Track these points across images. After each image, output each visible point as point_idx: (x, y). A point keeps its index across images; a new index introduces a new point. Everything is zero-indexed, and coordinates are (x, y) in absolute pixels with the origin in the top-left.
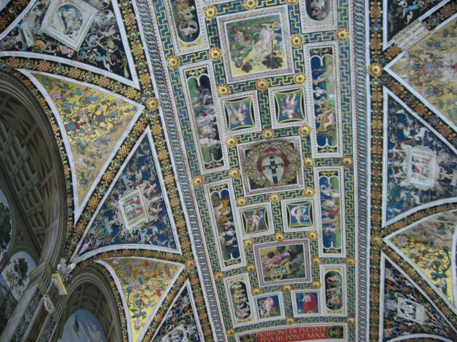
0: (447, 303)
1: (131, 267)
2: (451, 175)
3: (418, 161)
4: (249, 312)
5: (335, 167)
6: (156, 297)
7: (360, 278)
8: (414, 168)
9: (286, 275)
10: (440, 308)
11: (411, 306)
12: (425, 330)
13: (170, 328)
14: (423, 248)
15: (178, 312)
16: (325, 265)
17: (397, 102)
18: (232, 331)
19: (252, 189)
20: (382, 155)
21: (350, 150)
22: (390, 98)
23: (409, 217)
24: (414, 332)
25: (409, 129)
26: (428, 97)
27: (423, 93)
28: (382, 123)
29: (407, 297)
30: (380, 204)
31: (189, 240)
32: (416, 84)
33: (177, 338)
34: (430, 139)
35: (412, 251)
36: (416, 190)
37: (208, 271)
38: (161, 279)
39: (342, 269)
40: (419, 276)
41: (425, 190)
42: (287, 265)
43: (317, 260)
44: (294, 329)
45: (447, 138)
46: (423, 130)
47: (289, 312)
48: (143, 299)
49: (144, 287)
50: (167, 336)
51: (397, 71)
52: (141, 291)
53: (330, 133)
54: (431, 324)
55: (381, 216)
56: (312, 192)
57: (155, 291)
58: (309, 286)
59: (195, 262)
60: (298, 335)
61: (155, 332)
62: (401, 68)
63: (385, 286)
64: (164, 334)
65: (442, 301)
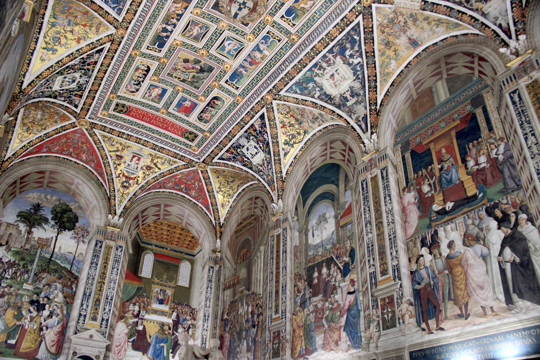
0: (282, 163)
1: (71, 8)
2: (351, 98)
3: (338, 74)
4: (137, 90)
5: (282, 36)
6: (74, 43)
7: (236, 113)
8: (332, 75)
9: (186, 80)
10: (275, 163)
11: (256, 150)
12: (254, 169)
13: (69, 72)
14: (293, 122)
15: (84, 62)
16: (219, 91)
17: (360, 31)
18: (115, 96)
19: (212, 8)
20: (320, 52)
21: (303, 34)
22: (358, 24)
23: (302, 100)
24: (245, 165)
25: (351, 52)
26: (380, 44)
27: (380, 39)
28: (339, 34)
29: (258, 144)
30: (291, 80)
31: (135, 15)
32: (381, 30)
33: (69, 82)
34: (358, 69)
35: (285, 119)
36: (322, 89)
37: (130, 46)
38: (88, 30)
39: (228, 100)
40: (277, 137)
41: (327, 93)
42: (192, 74)
43: (216, 84)
44: (162, 118)
45: (369, 77)
46: (359, 59)
47: (167, 105)
48: (61, 38)
49: (69, 29)
50: (63, 76)
51: (377, 13)
52: (65, 31)
53: (299, 13)
54: (261, 168)
55: (284, 87)
56: (252, 39)
57: (77, 38)
58: (197, 97)
59: (125, 33)
61: (57, 70)
62: (382, 13)
63: (249, 128)
64: (62, 74)
65: (280, 160)
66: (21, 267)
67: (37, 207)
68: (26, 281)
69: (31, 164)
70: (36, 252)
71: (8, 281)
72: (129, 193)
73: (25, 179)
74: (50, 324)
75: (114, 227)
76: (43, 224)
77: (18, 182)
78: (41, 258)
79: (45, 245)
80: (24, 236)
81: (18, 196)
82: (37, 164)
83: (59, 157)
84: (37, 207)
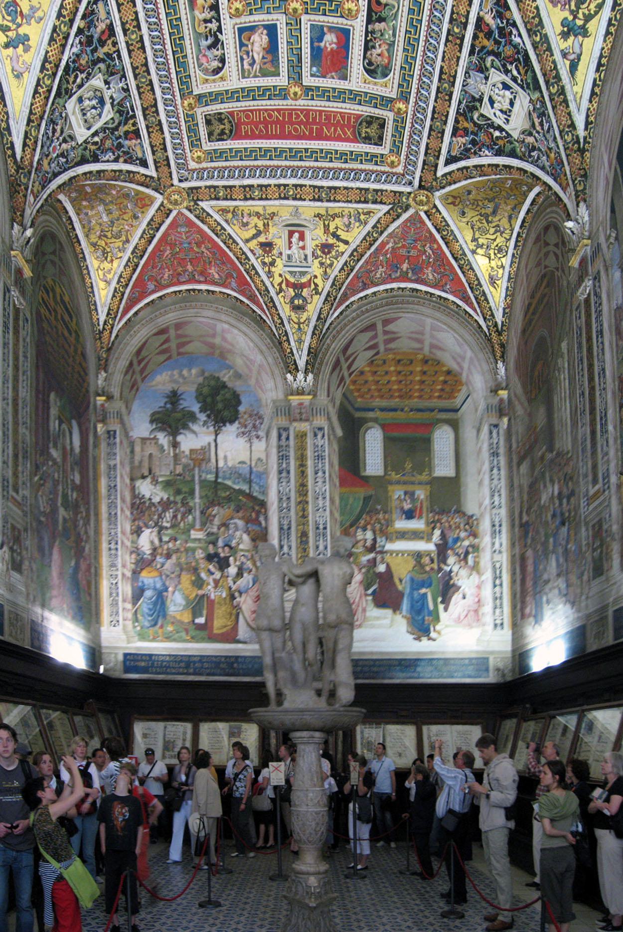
60: (305, 125)
66: (179, 505)
67: (174, 397)
68: (192, 526)
69: (144, 322)
70: (193, 476)
71: (169, 531)
72: (308, 319)
73: (144, 353)
74: (242, 585)
75: (298, 394)
76: (190, 425)
77: (135, 363)
78: (203, 482)
79: (202, 460)
80: (169, 453)
81: (142, 386)
82: (152, 320)
83: (180, 291)
84: (174, 397)
